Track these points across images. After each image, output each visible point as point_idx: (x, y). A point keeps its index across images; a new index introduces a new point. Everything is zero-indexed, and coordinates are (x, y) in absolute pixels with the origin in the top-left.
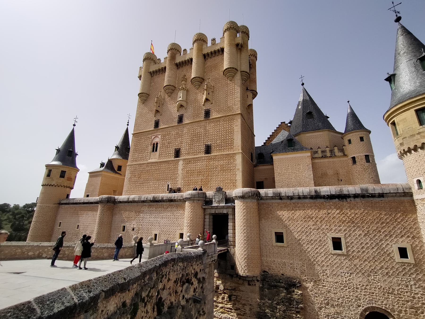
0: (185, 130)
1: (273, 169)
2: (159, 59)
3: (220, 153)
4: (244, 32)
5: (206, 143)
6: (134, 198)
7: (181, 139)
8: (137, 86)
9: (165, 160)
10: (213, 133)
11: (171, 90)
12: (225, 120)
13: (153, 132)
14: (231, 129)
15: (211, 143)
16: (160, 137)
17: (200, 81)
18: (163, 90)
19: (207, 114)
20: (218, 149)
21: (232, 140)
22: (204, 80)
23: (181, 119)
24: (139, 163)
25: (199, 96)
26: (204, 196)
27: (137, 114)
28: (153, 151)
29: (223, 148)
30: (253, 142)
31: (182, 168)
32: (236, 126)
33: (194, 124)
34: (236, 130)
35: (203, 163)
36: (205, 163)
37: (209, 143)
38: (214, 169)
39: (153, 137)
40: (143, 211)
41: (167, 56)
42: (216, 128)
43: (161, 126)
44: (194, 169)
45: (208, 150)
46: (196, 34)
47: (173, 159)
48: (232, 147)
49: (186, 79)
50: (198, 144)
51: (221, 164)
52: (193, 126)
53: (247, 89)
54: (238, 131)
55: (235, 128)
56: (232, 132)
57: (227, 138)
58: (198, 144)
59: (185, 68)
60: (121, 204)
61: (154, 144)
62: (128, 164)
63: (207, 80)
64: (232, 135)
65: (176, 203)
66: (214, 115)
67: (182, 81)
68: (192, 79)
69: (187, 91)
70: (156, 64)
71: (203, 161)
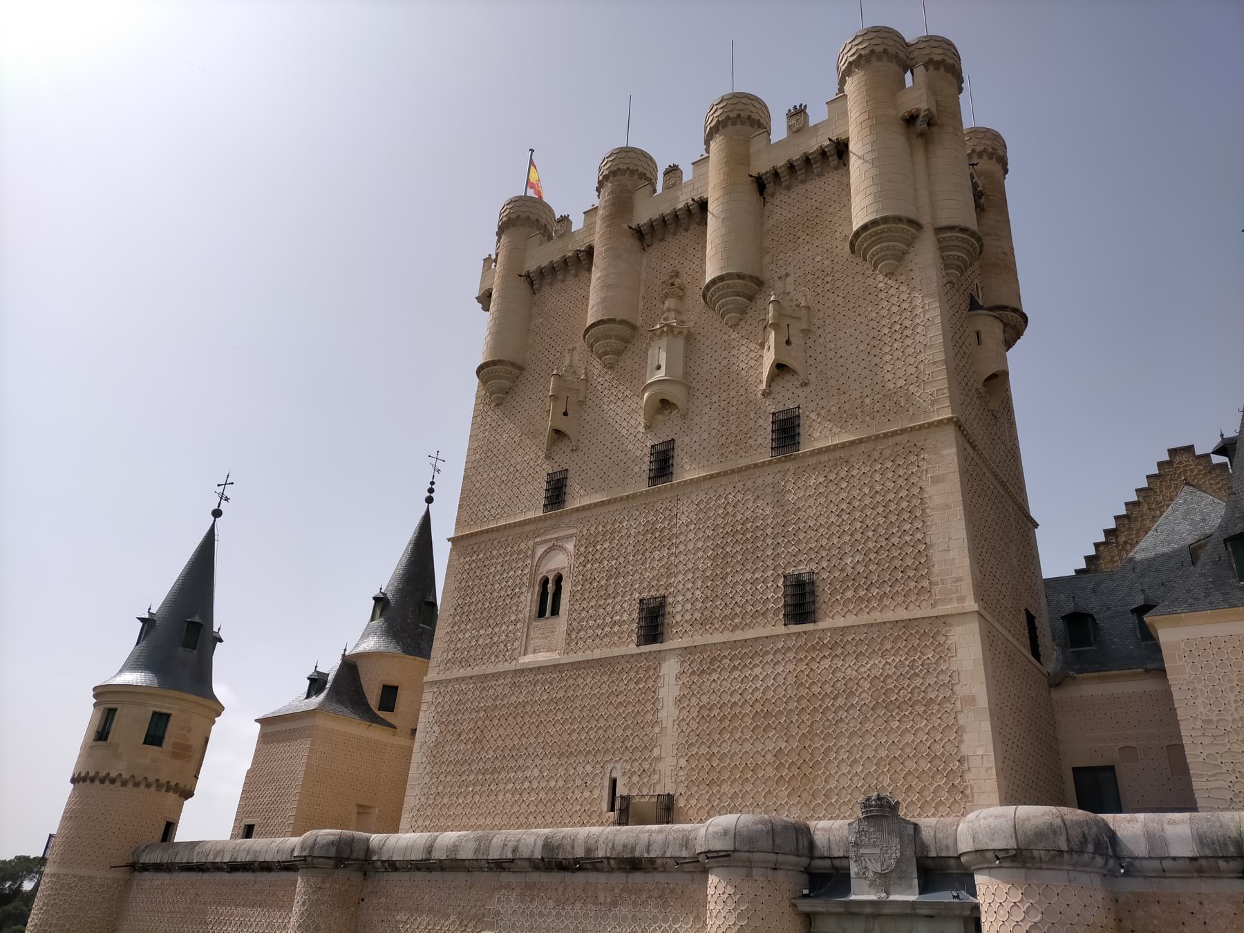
0: (686, 512)
1: (1168, 695)
2: (565, 220)
3: (864, 619)
4: (937, 65)
5: (790, 570)
6: (455, 847)
7: (665, 552)
8: (472, 336)
9: (597, 654)
10: (822, 520)
11: (618, 339)
12: (876, 455)
13: (541, 525)
14: (910, 498)
15: (813, 566)
16: (570, 546)
17: (744, 290)
18: (580, 345)
19: (787, 432)
20: (849, 594)
21: (922, 552)
22: (760, 283)
23: (663, 464)
24: (477, 671)
25: (742, 357)
26: (804, 843)
27: (472, 451)
28: (541, 614)
29: (875, 591)
30: (1030, 556)
31: (676, 692)
32: (937, 480)
33: (723, 481)
34: (937, 501)
35: (780, 669)
36: (791, 667)
37: (804, 569)
38: (841, 701)
39: (540, 551)
40: (498, 913)
41: (597, 202)
42: (832, 497)
43: (577, 498)
44: (737, 697)
45: (801, 602)
46: (715, 98)
47: (633, 649)
48: (925, 583)
49: (682, 288)
50: (748, 576)
51: (875, 672)
52: (721, 491)
53: (974, 305)
54: (947, 507)
55: (931, 490)
56: (916, 511)
57: (895, 540)
58: (748, 576)
59: (674, 245)
60: (395, 875)
61: (545, 582)
62: (432, 675)
63: (779, 284)
64: (918, 524)
65: (660, 877)
66: (819, 435)
67: (666, 296)
68: (708, 287)
69: (689, 338)
70: (550, 238)
71: (779, 657)
